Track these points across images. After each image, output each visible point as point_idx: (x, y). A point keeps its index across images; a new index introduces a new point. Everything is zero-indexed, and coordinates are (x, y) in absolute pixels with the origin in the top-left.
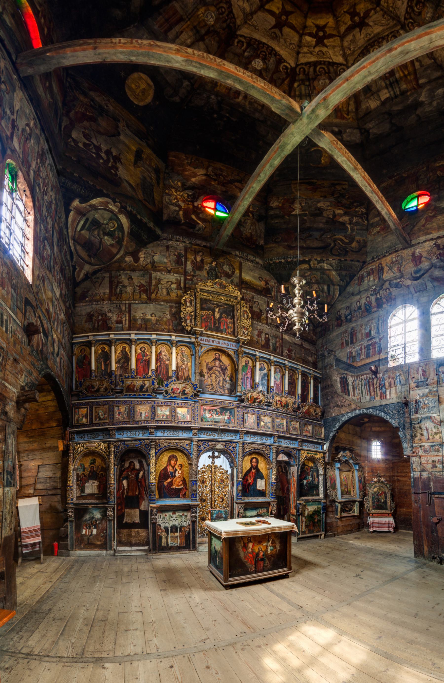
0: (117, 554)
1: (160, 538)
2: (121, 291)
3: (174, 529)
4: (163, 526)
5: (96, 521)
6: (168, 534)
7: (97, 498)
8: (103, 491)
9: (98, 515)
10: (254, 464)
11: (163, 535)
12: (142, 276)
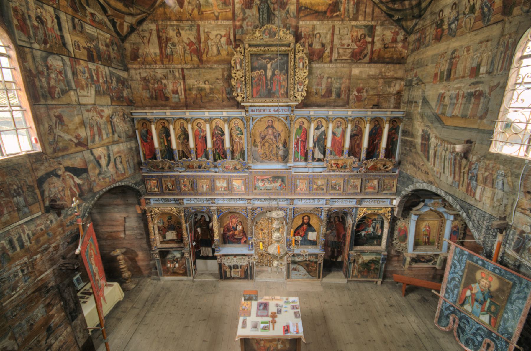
0: (195, 280)
1: (225, 272)
2: (172, 51)
3: (236, 267)
4: (227, 265)
5: (177, 259)
6: (231, 269)
7: (177, 243)
8: (180, 239)
9: (178, 255)
10: (305, 221)
11: (228, 270)
12: (189, 29)
